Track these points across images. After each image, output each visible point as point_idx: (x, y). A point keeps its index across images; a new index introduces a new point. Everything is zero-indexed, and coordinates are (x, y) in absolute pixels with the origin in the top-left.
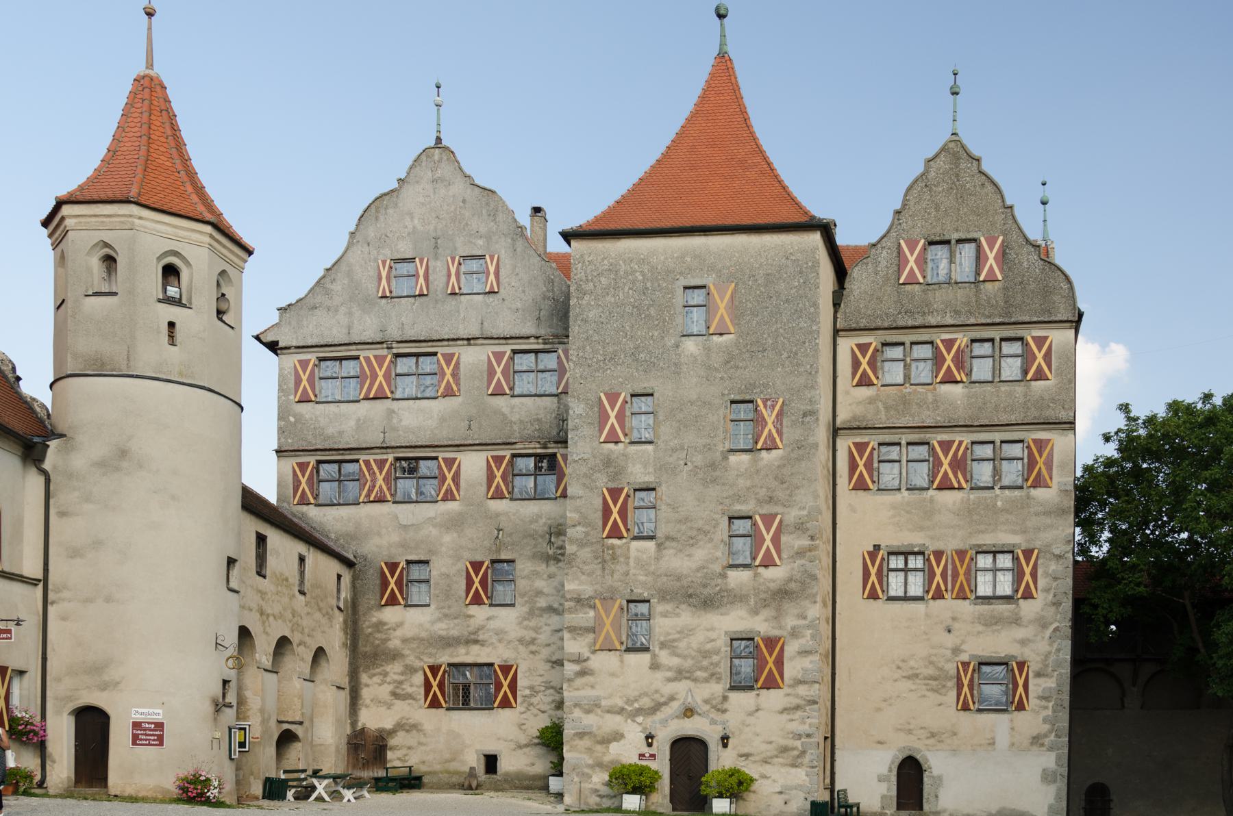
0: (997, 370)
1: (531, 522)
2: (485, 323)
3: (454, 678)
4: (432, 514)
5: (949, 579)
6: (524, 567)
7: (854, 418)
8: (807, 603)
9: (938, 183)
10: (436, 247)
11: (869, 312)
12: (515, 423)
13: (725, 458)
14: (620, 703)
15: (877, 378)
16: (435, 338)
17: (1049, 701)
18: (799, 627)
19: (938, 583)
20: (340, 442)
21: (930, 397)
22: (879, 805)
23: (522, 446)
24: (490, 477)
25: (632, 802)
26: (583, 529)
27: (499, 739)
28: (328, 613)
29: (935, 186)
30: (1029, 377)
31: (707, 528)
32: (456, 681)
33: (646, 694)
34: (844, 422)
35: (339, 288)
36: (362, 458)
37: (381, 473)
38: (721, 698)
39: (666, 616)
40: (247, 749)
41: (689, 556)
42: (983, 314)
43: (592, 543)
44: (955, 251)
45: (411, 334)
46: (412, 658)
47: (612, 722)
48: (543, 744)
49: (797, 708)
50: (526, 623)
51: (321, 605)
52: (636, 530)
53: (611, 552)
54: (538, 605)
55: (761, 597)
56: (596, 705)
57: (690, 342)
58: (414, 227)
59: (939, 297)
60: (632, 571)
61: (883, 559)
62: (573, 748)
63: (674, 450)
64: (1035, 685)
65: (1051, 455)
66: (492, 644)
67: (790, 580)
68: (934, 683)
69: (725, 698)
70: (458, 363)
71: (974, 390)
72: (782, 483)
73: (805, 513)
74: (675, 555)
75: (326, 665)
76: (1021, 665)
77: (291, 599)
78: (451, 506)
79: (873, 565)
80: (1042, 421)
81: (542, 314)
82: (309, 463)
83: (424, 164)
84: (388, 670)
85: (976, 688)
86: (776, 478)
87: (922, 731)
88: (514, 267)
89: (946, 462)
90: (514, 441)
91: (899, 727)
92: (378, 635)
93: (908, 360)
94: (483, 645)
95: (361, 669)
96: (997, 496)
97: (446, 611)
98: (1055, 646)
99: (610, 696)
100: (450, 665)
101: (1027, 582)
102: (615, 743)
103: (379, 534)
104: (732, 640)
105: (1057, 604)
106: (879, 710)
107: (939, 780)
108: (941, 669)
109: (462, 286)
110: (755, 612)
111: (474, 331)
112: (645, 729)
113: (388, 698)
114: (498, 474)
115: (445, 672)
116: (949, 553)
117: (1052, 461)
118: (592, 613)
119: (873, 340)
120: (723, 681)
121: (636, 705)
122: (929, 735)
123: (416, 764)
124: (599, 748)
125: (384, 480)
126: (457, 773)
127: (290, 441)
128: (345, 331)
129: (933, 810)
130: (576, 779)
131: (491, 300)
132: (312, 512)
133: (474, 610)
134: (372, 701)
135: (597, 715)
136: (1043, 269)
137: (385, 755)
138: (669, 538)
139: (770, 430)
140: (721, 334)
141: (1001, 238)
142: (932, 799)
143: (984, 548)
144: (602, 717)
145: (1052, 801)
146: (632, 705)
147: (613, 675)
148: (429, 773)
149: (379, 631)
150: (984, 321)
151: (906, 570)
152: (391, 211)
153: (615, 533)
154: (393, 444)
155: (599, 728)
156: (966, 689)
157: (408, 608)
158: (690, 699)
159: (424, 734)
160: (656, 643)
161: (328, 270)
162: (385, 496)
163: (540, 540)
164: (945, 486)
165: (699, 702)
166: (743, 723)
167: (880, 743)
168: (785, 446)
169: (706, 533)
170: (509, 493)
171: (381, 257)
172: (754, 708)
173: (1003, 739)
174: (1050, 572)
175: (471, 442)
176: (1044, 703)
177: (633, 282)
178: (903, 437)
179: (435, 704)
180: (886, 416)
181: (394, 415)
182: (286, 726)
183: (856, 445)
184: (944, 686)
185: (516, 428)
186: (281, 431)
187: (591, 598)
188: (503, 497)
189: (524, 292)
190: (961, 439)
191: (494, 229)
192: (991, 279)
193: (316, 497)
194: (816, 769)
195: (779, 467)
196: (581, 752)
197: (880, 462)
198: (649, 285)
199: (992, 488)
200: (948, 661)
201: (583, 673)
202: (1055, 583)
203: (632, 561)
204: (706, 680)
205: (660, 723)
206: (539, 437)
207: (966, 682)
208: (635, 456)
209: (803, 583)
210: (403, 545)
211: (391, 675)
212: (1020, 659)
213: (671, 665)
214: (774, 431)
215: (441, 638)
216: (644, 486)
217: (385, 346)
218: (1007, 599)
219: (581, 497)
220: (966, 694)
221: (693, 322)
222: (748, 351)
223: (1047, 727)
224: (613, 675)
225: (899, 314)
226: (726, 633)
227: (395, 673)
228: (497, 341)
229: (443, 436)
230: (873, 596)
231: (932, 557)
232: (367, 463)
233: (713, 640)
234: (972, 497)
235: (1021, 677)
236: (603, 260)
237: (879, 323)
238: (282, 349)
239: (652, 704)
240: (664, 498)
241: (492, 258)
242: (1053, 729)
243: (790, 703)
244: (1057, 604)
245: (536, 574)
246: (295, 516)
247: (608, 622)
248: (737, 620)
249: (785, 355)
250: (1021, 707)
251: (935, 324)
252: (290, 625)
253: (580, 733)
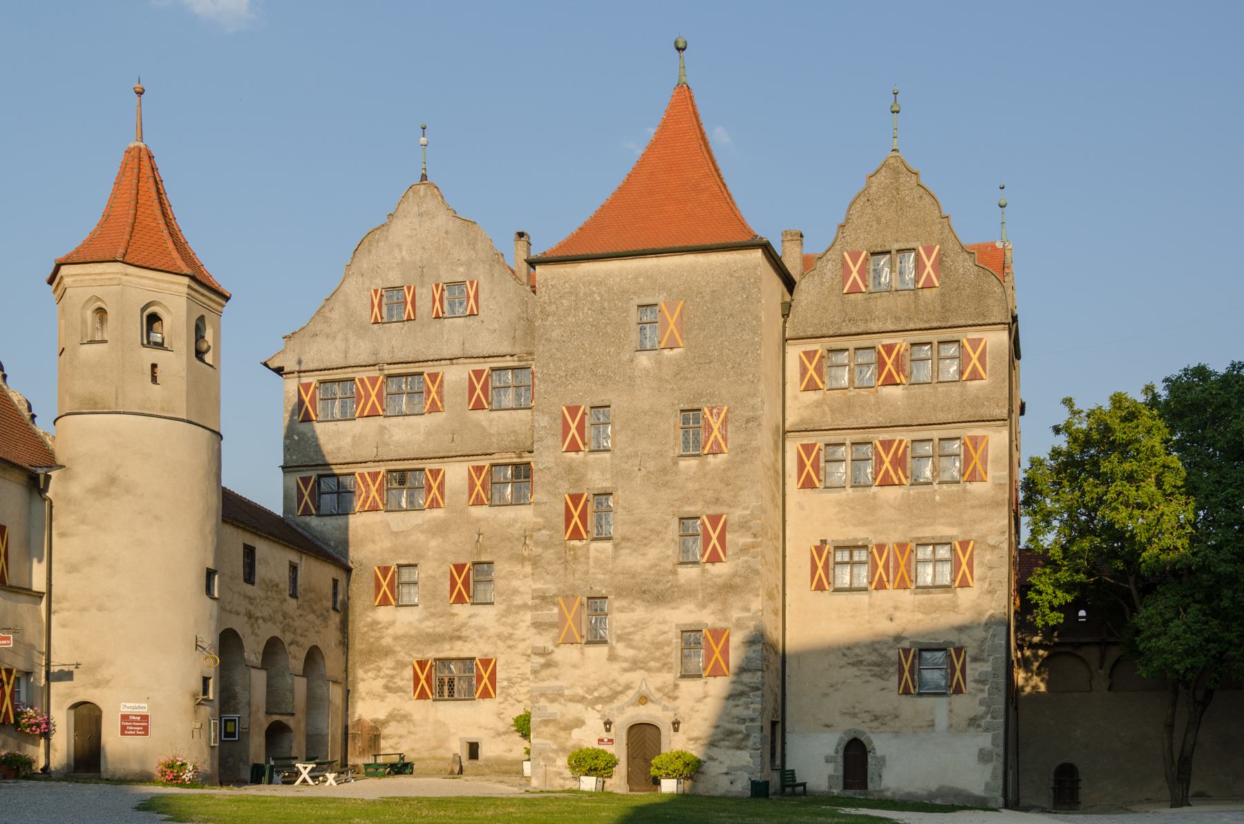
0: (937, 371)
1: (508, 526)
2: (467, 345)
3: (441, 672)
4: (420, 521)
5: (891, 570)
6: (501, 568)
7: (802, 421)
8: (750, 596)
9: (880, 197)
10: (422, 275)
11: (816, 321)
12: (493, 435)
13: (676, 463)
14: (581, 692)
15: (823, 383)
16: (421, 359)
17: (985, 685)
18: (743, 618)
19: (881, 575)
21: (872, 400)
22: (827, 785)
23: (500, 457)
24: (472, 486)
25: (589, 783)
26: (548, 533)
27: (480, 727)
28: (322, 615)
29: (876, 200)
30: (964, 378)
31: (659, 528)
32: (442, 675)
33: (604, 684)
34: (792, 425)
35: (337, 316)
36: (358, 470)
37: (374, 484)
38: (672, 686)
39: (622, 611)
40: (237, 739)
41: (644, 555)
42: (922, 320)
43: (556, 545)
44: (896, 260)
45: (400, 356)
46: (402, 654)
47: (575, 710)
48: (518, 731)
49: (742, 694)
50: (504, 619)
51: (315, 607)
52: (595, 531)
53: (572, 553)
54: (515, 603)
55: (708, 591)
56: (560, 695)
57: (643, 357)
58: (402, 258)
59: (882, 304)
60: (592, 571)
61: (829, 552)
62: (539, 735)
63: (629, 457)
64: (972, 669)
65: (986, 449)
66: (474, 639)
67: (735, 575)
68: (876, 669)
69: (676, 686)
70: (442, 381)
71: (913, 391)
72: (727, 485)
73: (748, 512)
74: (630, 554)
76: (959, 650)
77: (281, 603)
78: (437, 513)
79: (820, 559)
80: (977, 419)
81: (517, 334)
82: (311, 477)
83: (411, 199)
84: (381, 665)
85: (916, 673)
86: (722, 481)
87: (866, 714)
88: (492, 291)
89: (887, 460)
90: (493, 452)
91: (845, 711)
92: (373, 634)
93: (852, 364)
94: (465, 641)
95: (358, 665)
96: (935, 491)
97: (432, 610)
98: (991, 632)
99: (572, 686)
100: (436, 660)
101: (964, 572)
102: (576, 730)
103: (373, 541)
104: (682, 632)
105: (991, 592)
106: (826, 695)
107: (882, 761)
108: (883, 656)
109: (445, 310)
110: (703, 606)
111: (455, 350)
112: (604, 716)
113: (380, 690)
114: (479, 483)
115: (431, 666)
116: (891, 546)
117: (987, 456)
118: (556, 610)
119: (818, 346)
120: (674, 671)
121: (596, 694)
122: (873, 718)
123: (406, 751)
124: (562, 734)
125: (377, 490)
126: (443, 759)
127: (295, 458)
128: (342, 355)
129: (877, 789)
130: (542, 763)
131: (471, 322)
132: (314, 522)
133: (458, 608)
134: (367, 694)
135: (561, 704)
136: (978, 274)
137: (379, 743)
138: (625, 539)
139: (716, 436)
140: (671, 348)
141: (938, 247)
142: (876, 778)
143: (924, 541)
144: (565, 705)
145: (989, 779)
146: (590, 695)
147: (575, 666)
148: (419, 760)
149: (373, 630)
150: (922, 326)
151: (852, 563)
152: (382, 244)
153: (576, 535)
154: (385, 458)
155: (563, 715)
156: (907, 674)
157: (398, 608)
158: (644, 688)
159: (414, 725)
160: (614, 636)
162: (378, 506)
163: (517, 543)
164: (886, 482)
165: (653, 690)
166: (692, 709)
167: (827, 726)
168: (730, 450)
169: (658, 533)
170: (488, 500)
171: (374, 287)
172: (701, 695)
173: (942, 720)
174: (986, 561)
175: (454, 454)
176: (980, 686)
177: (592, 303)
178: (848, 437)
179: (422, 696)
180: (832, 418)
181: (386, 431)
182: (276, 718)
183: (803, 446)
184: (887, 672)
185: (494, 439)
186: (287, 449)
187: (555, 596)
188: (482, 504)
189: (501, 313)
190: (901, 438)
191: (474, 257)
192: (929, 285)
193: (318, 508)
194: (759, 751)
195: (724, 470)
196: (545, 738)
197: (826, 461)
198: (606, 305)
199: (931, 484)
200: (891, 648)
201: (548, 665)
202: (990, 574)
203: (591, 562)
204: (659, 670)
205: (617, 710)
206: (515, 447)
207: (907, 667)
208: (594, 464)
209: (746, 578)
210: (395, 551)
211: (384, 670)
212: (957, 645)
213: (627, 656)
214: (719, 437)
215: (428, 635)
216: (602, 492)
217: (377, 367)
218: (945, 588)
219: (546, 503)
220: (907, 679)
221: (646, 338)
222: (696, 363)
223: (983, 709)
224: (575, 666)
225: (843, 322)
226: (677, 625)
227: (387, 668)
228: (477, 360)
229: (430, 449)
230: (820, 587)
231: (875, 550)
232: (362, 475)
233: (665, 633)
234: (912, 492)
235: (958, 662)
236: (564, 283)
237: (825, 331)
238: (286, 374)
239: (610, 693)
240: (620, 501)
241: (472, 283)
242: (989, 711)
243: (736, 690)
244: (991, 592)
245: (512, 574)
246: (298, 525)
247: (570, 617)
248: (685, 614)
249: (730, 365)
250: (958, 690)
251: (877, 330)
252: (282, 626)
253: (546, 721)
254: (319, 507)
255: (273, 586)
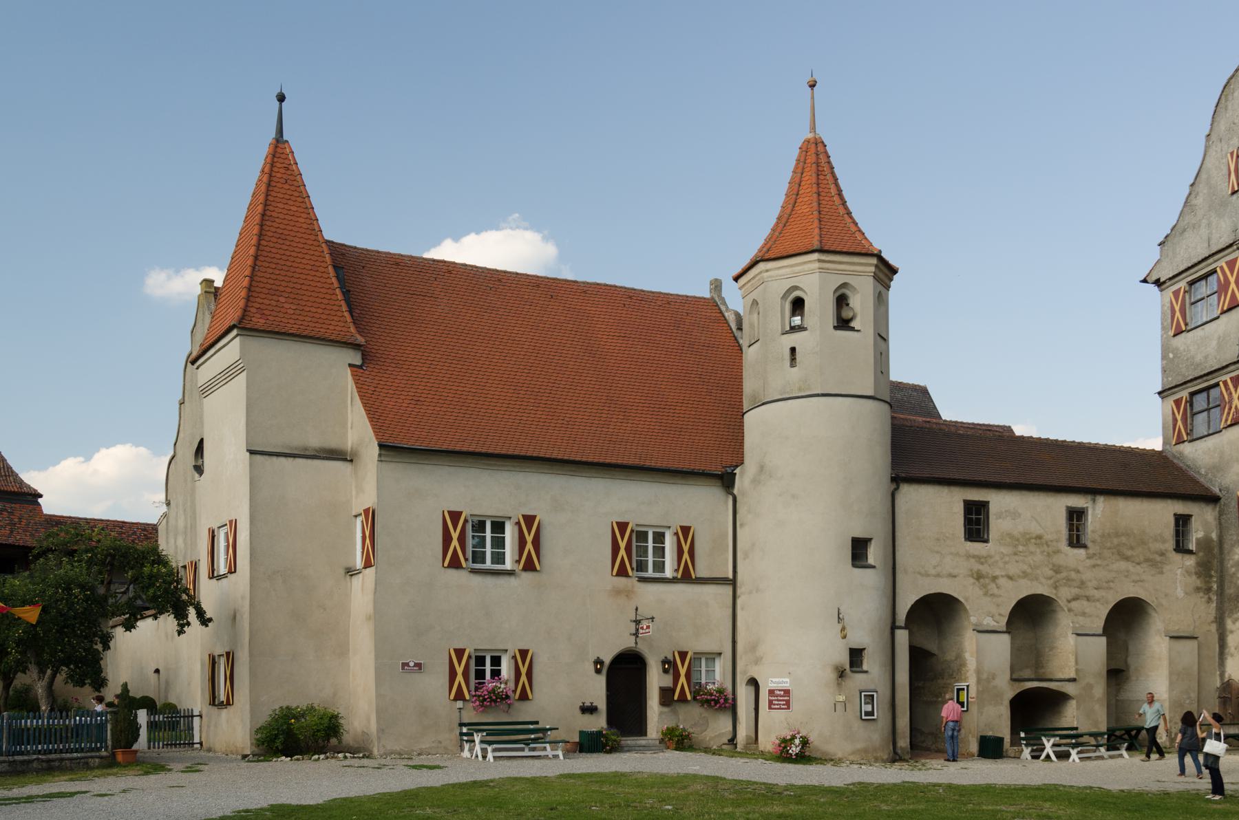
20: (1206, 367)
75: (1156, 615)
95: (1226, 615)
128: (1206, 245)
134: (1236, 649)
161: (1192, 185)
254: (1191, 430)
255: (1029, 539)
